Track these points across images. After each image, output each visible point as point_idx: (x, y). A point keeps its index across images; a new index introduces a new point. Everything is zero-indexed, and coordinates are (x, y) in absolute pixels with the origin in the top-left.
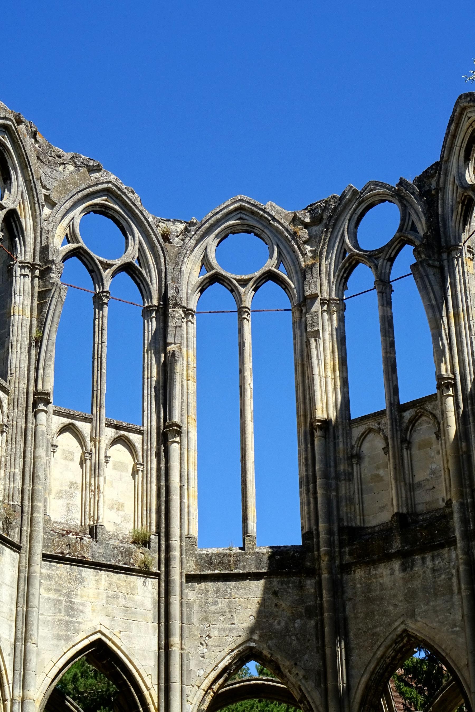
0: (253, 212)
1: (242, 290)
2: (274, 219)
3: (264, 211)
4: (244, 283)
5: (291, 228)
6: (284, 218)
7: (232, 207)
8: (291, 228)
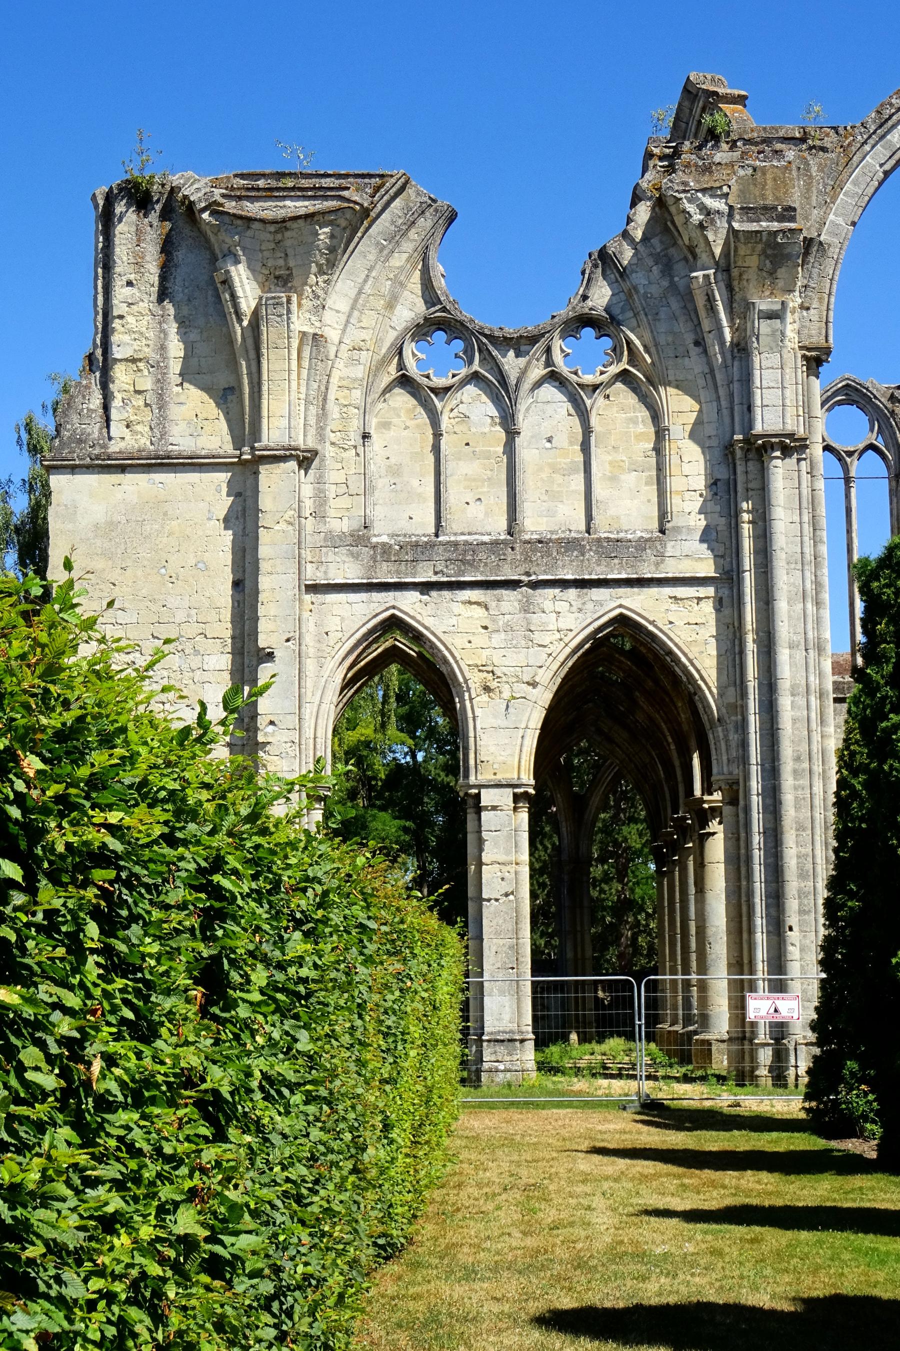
0: (857, 389)
1: (848, 460)
2: (875, 397)
3: (867, 389)
4: (850, 454)
5: (890, 405)
6: (883, 395)
7: (840, 385)
8: (890, 405)
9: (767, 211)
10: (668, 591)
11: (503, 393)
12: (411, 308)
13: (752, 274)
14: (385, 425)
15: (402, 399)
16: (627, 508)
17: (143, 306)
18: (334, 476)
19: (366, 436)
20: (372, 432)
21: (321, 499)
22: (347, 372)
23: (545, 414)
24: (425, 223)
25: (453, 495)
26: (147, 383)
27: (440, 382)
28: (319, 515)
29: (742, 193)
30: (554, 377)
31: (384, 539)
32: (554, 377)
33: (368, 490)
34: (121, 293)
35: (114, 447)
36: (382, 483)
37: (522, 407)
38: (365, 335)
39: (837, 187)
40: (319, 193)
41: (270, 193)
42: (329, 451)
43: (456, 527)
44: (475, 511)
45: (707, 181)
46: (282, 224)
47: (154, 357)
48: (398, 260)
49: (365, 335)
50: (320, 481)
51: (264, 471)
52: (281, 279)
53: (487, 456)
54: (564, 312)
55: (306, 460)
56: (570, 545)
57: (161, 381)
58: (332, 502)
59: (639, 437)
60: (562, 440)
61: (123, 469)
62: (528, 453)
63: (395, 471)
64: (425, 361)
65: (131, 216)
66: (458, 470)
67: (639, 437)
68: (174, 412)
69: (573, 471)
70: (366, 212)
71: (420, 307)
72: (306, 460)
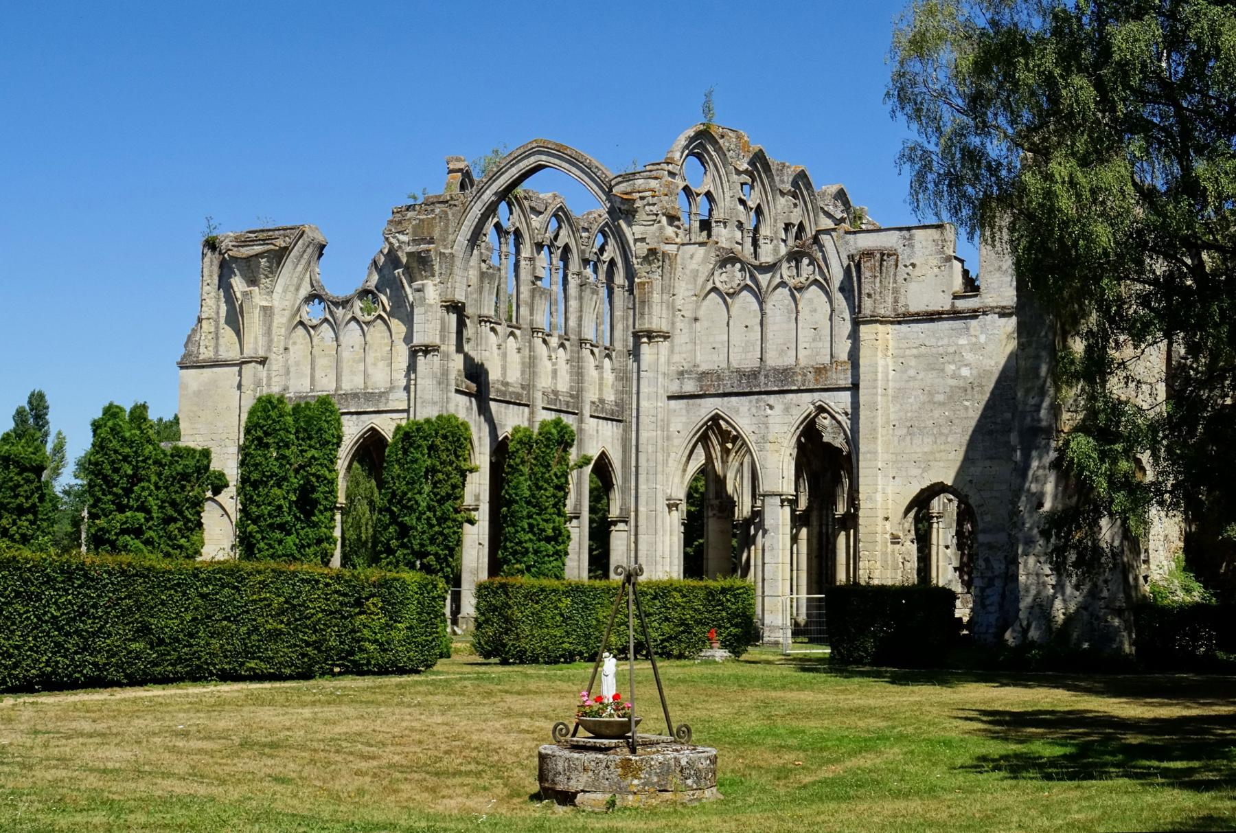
9: (423, 241)
10: (389, 415)
11: (335, 326)
12: (305, 290)
13: (416, 270)
14: (294, 343)
15: (300, 329)
16: (379, 379)
17: (213, 294)
18: (275, 367)
19: (286, 349)
20: (290, 347)
21: (269, 378)
22: (280, 320)
23: (352, 334)
24: (309, 250)
25: (318, 375)
26: (213, 329)
27: (315, 322)
28: (269, 385)
29: (415, 233)
30: (354, 318)
31: (291, 395)
32: (354, 318)
33: (288, 372)
34: (206, 288)
35: (201, 357)
36: (292, 369)
37: (341, 334)
38: (287, 303)
39: (460, 224)
40: (264, 241)
41: (252, 242)
42: (272, 356)
43: (318, 388)
44: (325, 380)
45: (400, 228)
46: (248, 259)
47: (213, 315)
48: (300, 268)
49: (287, 303)
50: (269, 370)
51: (244, 366)
52: (253, 282)
53: (330, 355)
54: (359, 286)
55: (263, 362)
56: (355, 395)
57: (217, 328)
58: (274, 379)
59: (386, 345)
60: (357, 348)
61: (203, 367)
62: (346, 354)
63: (297, 364)
64: (314, 313)
65: (209, 254)
66: (322, 362)
67: (386, 345)
68: (221, 341)
69: (359, 361)
70: (286, 248)
71: (309, 289)
72: (263, 362)
